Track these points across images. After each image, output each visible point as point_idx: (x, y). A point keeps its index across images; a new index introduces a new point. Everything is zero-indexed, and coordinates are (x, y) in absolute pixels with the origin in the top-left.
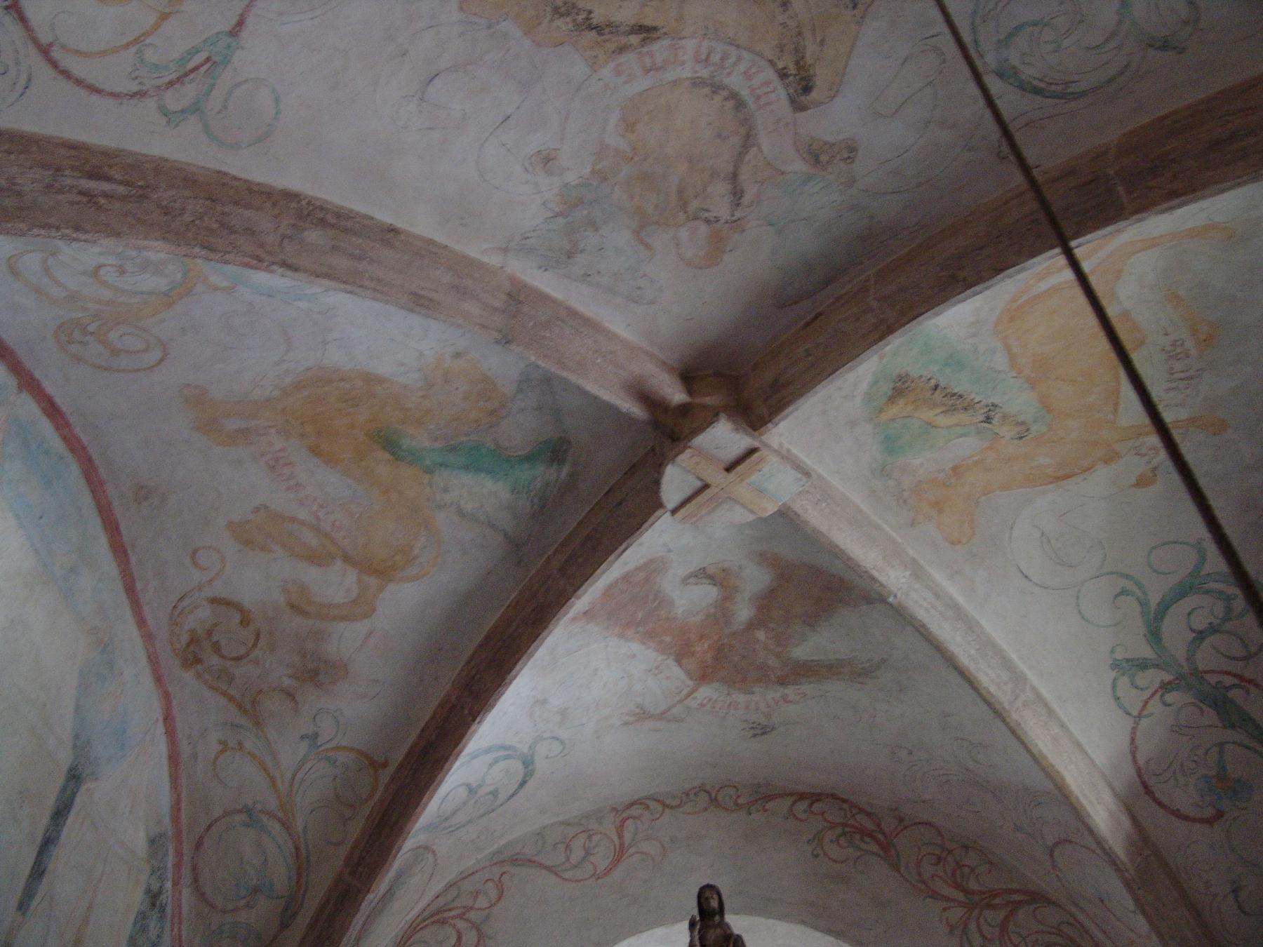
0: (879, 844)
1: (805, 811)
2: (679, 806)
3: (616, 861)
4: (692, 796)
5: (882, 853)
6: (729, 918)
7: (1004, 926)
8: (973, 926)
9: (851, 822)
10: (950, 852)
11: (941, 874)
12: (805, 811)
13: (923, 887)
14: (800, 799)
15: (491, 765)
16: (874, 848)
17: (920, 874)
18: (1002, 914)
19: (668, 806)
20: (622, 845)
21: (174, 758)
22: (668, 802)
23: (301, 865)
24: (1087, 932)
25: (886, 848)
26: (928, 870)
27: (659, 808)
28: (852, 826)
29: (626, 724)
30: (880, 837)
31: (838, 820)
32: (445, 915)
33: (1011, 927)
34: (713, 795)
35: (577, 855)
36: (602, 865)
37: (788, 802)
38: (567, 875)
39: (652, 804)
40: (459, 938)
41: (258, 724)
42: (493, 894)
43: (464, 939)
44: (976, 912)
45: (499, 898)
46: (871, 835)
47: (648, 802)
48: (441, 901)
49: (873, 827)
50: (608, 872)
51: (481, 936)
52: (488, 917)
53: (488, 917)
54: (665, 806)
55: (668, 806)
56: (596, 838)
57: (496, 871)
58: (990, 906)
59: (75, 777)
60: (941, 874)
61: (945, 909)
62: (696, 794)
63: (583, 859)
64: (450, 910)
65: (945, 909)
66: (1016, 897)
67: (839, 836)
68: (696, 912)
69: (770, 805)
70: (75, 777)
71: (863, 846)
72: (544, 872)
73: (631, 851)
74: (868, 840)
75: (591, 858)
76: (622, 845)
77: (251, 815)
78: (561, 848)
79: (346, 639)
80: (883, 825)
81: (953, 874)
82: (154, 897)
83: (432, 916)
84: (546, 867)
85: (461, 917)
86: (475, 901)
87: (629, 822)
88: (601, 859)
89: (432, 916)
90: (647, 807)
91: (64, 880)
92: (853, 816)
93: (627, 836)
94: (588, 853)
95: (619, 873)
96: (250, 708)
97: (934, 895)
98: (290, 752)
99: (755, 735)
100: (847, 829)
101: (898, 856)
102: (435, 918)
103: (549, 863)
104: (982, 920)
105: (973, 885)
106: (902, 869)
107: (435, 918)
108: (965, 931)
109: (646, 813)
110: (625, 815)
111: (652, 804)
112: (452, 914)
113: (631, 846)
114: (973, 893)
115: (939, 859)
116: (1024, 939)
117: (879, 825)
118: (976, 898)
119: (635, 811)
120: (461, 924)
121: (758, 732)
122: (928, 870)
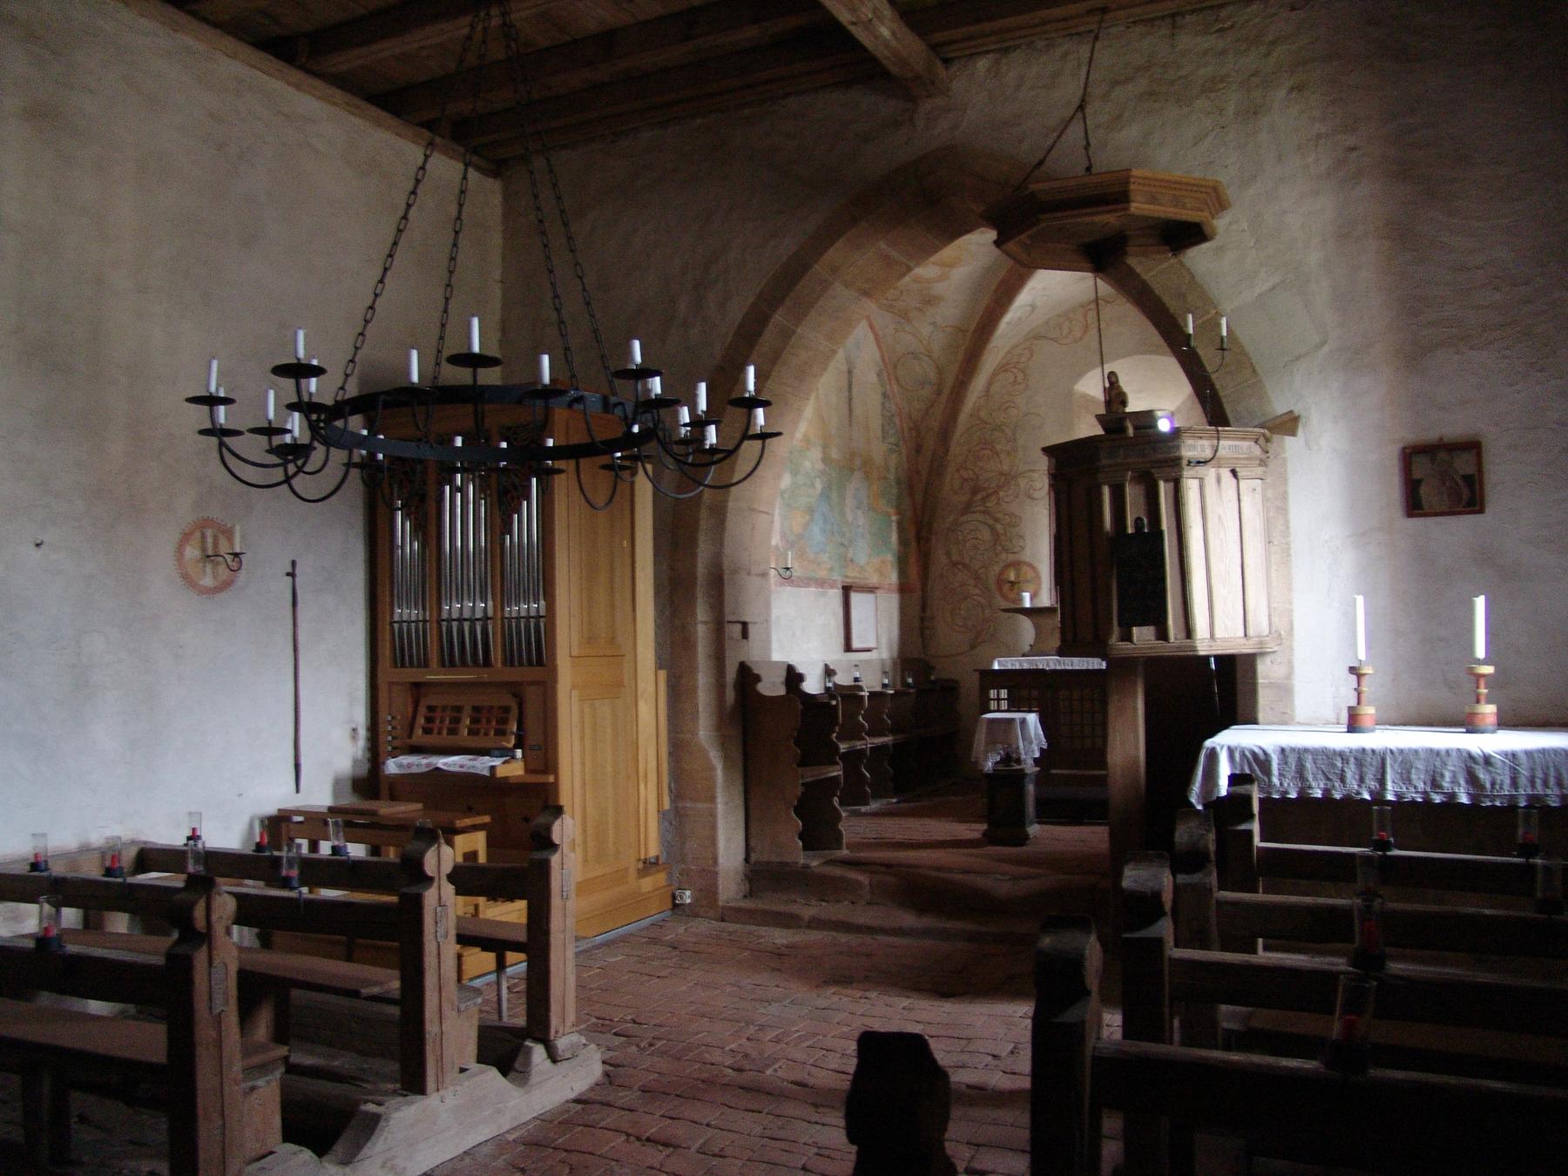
3: (1085, 333)
6: (1121, 383)
21: (877, 339)
23: (940, 371)
35: (1065, 331)
36: (1078, 335)
41: (909, 321)
59: (850, 372)
70: (850, 372)
77: (915, 355)
79: (939, 289)
82: (885, 395)
91: (858, 411)
96: (905, 316)
98: (926, 330)
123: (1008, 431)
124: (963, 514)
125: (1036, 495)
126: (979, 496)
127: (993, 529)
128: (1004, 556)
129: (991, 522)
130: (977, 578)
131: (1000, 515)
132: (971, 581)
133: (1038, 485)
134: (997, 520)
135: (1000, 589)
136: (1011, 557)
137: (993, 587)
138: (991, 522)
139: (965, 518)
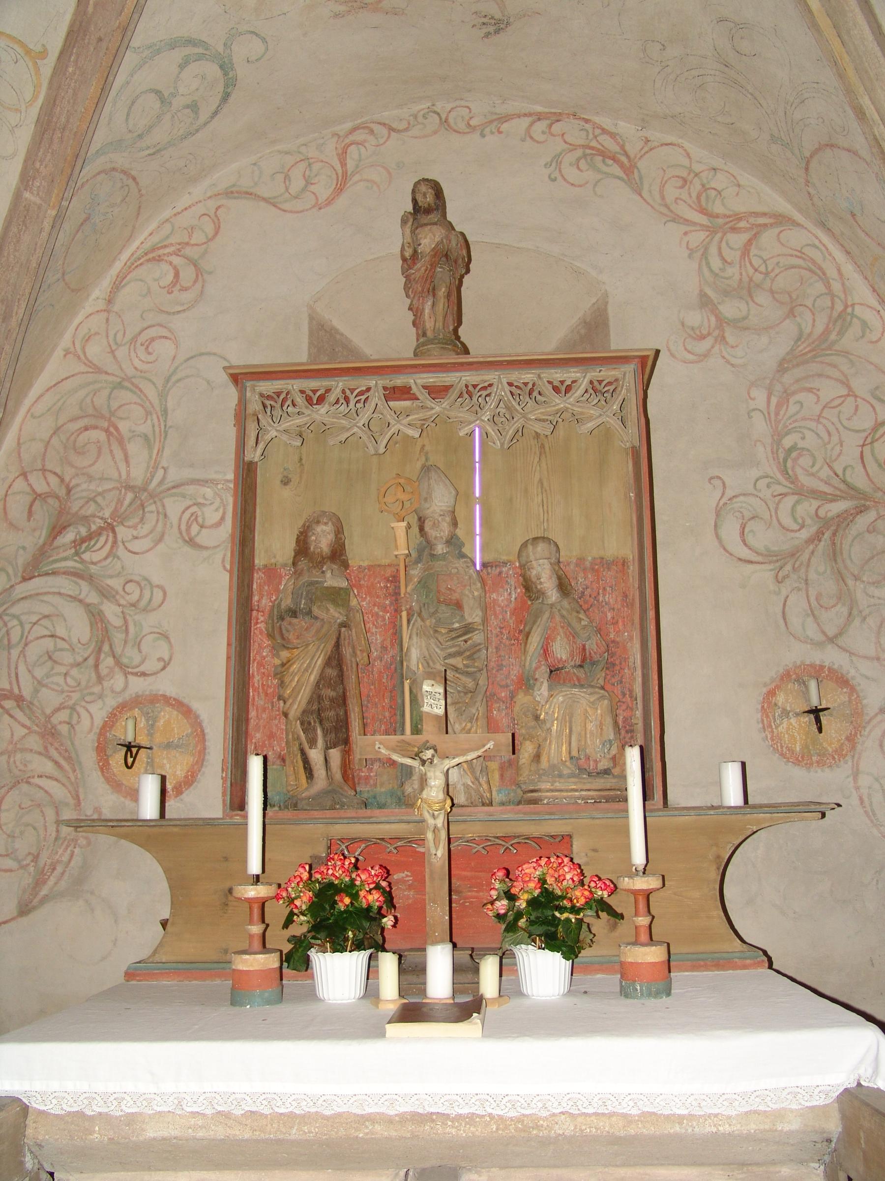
0: (622, 166)
1: (543, 133)
2: (406, 130)
3: (340, 189)
4: (420, 119)
5: (625, 177)
7: (745, 251)
8: (713, 250)
9: (594, 144)
10: (696, 175)
11: (685, 196)
12: (543, 133)
13: (664, 210)
14: (539, 119)
15: (182, 67)
16: (617, 170)
17: (663, 198)
18: (744, 237)
19: (394, 130)
20: (345, 173)
22: (394, 126)
24: (830, 254)
25: (629, 169)
26: (671, 192)
27: (385, 132)
28: (592, 148)
29: (336, 16)
30: (624, 159)
31: (581, 142)
32: (161, 252)
33: (753, 251)
34: (444, 117)
35: (297, 184)
37: (525, 122)
38: (286, 206)
39: (377, 128)
40: (177, 275)
42: (209, 229)
43: (181, 275)
44: (719, 235)
45: (216, 233)
46: (614, 159)
47: (372, 125)
48: (155, 239)
49: (617, 149)
50: (329, 202)
51: (199, 272)
52: (206, 252)
53: (206, 252)
54: (391, 129)
55: (394, 130)
56: (316, 167)
57: (212, 204)
58: (734, 229)
60: (685, 196)
61: (686, 233)
62: (424, 117)
63: (304, 189)
64: (165, 246)
65: (686, 233)
66: (761, 220)
67: (578, 160)
68: (410, 208)
69: (505, 127)
71: (605, 169)
72: (262, 204)
73: (356, 178)
74: (610, 162)
75: (312, 188)
76: (345, 173)
78: (280, 177)
80: (628, 148)
81: (699, 197)
83: (146, 254)
84: (264, 199)
85: (176, 253)
86: (190, 237)
87: (353, 147)
88: (323, 188)
89: (146, 254)
90: (372, 132)
92: (596, 137)
93: (350, 165)
94: (308, 182)
95: (342, 201)
97: (676, 219)
99: (487, 35)
100: (588, 151)
101: (641, 178)
102: (151, 256)
103: (266, 195)
104: (724, 245)
105: (718, 209)
106: (645, 194)
107: (151, 256)
108: (705, 255)
109: (372, 140)
110: (347, 141)
111: (377, 128)
112: (167, 251)
113: (353, 174)
114: (717, 216)
115: (685, 181)
116: (765, 262)
117: (622, 147)
118: (720, 221)
119: (359, 136)
120: (176, 260)
121: (491, 29)
122: (671, 192)
123: (152, 393)
124: (25, 579)
125: (205, 538)
126: (69, 536)
127: (96, 617)
128: (118, 681)
129: (93, 598)
130: (50, 733)
131: (115, 583)
132: (34, 742)
133: (211, 515)
134: (106, 594)
135: (104, 766)
136: (138, 686)
137: (89, 758)
138: (93, 598)
139: (23, 589)
